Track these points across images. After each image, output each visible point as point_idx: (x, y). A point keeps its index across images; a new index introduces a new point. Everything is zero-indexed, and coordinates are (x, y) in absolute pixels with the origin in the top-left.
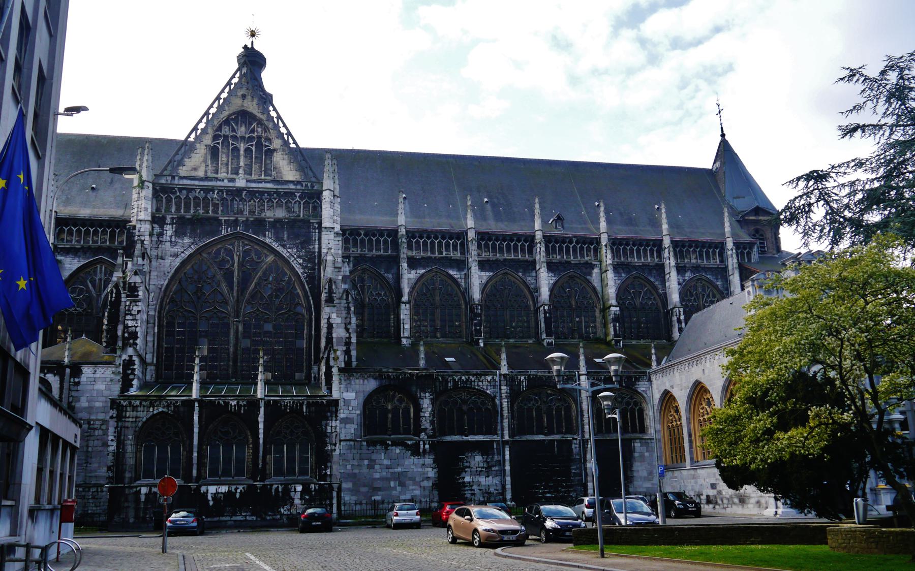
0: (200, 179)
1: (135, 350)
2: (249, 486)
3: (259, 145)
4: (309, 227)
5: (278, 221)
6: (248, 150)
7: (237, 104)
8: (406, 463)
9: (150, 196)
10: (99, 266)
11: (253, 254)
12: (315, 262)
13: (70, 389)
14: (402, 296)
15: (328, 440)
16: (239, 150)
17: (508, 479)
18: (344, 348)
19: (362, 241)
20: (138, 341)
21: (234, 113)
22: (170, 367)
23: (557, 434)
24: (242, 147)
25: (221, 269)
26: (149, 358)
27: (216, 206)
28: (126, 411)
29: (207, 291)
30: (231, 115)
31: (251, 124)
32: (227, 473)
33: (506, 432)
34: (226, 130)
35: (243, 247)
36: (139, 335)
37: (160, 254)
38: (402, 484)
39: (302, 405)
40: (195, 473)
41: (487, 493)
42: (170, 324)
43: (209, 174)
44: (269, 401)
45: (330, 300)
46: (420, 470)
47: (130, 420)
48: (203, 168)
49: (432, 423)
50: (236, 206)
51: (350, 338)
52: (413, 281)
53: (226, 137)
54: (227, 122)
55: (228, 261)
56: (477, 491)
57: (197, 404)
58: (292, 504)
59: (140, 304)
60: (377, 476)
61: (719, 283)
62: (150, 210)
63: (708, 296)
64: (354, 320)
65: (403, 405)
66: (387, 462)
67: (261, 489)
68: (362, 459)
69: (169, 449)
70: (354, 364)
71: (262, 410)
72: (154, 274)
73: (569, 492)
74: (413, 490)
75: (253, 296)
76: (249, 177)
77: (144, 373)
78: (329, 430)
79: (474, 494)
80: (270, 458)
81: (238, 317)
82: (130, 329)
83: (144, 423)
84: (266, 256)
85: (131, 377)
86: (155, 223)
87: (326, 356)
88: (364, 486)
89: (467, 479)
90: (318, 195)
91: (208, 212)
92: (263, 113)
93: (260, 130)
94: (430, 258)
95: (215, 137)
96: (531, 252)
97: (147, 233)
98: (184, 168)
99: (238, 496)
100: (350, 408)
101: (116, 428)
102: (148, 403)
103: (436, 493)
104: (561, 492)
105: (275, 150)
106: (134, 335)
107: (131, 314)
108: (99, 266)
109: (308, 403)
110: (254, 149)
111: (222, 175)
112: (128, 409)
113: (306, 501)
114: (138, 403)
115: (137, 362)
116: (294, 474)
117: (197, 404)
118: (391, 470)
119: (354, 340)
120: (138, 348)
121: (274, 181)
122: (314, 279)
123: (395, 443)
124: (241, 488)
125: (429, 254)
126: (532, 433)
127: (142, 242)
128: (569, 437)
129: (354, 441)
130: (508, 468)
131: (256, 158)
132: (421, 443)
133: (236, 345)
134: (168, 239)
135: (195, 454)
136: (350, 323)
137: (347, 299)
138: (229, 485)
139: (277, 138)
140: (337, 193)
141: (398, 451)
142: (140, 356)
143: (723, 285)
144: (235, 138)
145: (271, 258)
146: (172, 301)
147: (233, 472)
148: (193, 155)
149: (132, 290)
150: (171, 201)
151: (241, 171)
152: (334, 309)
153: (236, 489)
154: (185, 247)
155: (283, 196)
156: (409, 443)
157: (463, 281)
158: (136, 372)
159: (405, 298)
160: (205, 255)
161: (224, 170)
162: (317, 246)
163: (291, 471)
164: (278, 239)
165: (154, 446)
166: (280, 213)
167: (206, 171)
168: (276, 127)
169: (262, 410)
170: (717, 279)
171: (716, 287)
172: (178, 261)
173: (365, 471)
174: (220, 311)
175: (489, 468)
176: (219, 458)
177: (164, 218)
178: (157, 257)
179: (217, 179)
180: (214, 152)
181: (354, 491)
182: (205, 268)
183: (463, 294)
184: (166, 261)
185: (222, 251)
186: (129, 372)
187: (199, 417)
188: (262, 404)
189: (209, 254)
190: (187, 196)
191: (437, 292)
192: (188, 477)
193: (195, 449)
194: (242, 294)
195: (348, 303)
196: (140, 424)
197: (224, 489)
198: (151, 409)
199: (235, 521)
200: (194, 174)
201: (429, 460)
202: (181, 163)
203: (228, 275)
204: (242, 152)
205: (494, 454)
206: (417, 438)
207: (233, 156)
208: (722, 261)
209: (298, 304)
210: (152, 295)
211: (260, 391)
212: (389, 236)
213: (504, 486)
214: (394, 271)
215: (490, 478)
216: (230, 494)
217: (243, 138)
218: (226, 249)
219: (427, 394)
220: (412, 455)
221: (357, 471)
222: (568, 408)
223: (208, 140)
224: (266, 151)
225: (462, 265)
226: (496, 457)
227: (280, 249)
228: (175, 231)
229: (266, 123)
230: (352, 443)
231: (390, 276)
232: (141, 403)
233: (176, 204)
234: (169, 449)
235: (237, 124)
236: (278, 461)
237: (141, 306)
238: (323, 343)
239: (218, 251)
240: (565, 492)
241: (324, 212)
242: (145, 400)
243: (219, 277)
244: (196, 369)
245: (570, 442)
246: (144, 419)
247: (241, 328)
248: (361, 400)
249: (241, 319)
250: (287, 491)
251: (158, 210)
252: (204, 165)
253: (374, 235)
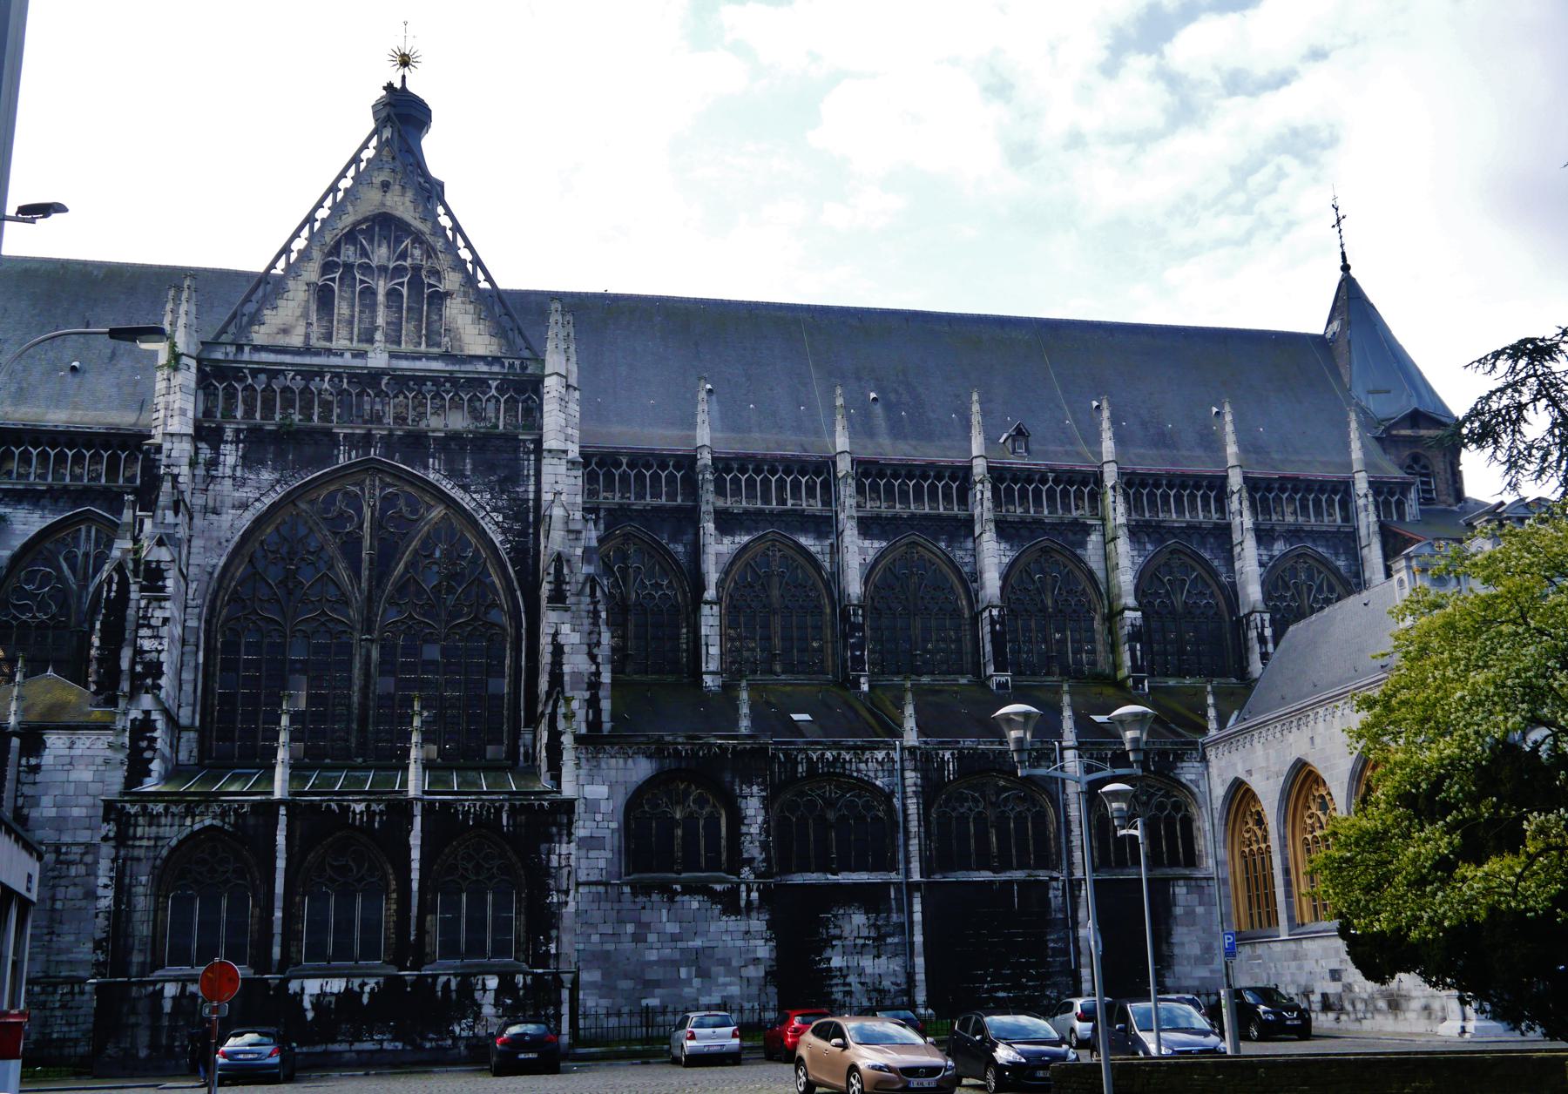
0: (296, 352)
1: (157, 698)
2: (388, 978)
3: (416, 284)
4: (516, 450)
5: (454, 437)
6: (393, 294)
7: (372, 201)
8: (712, 929)
9: (193, 385)
10: (83, 528)
11: (401, 503)
12: (528, 521)
13: (18, 781)
14: (704, 589)
15: (552, 882)
16: (374, 293)
17: (920, 961)
18: (587, 695)
19: (624, 478)
20: (163, 681)
21: (365, 220)
22: (230, 737)
23: (1020, 868)
24: (382, 287)
25: (335, 534)
26: (185, 715)
27: (326, 406)
28: (136, 825)
29: (307, 578)
30: (360, 222)
31: (399, 241)
32: (343, 952)
33: (915, 865)
34: (349, 254)
35: (382, 489)
36: (165, 668)
37: (211, 504)
38: (703, 974)
39: (499, 811)
40: (276, 952)
41: (875, 990)
42: (231, 646)
43: (314, 342)
44: (432, 803)
45: (558, 597)
46: (740, 943)
47: (145, 843)
48: (300, 330)
49: (764, 846)
50: (367, 407)
51: (598, 674)
52: (726, 559)
53: (348, 267)
54: (351, 236)
55: (351, 517)
56: (856, 987)
57: (283, 811)
58: (477, 1016)
59: (168, 604)
60: (652, 956)
62: (191, 414)
63: (1320, 589)
64: (606, 638)
65: (708, 809)
66: (673, 928)
67: (413, 984)
68: (621, 921)
69: (224, 903)
70: (607, 726)
71: (418, 821)
72: (195, 542)
73: (1043, 988)
74: (725, 985)
75: (401, 589)
76: (394, 347)
77: (175, 747)
78: (554, 863)
79: (849, 993)
80: (434, 922)
81: (369, 632)
82: (148, 657)
83: (173, 850)
84: (429, 508)
85: (148, 754)
86: (202, 440)
87: (549, 710)
88: (626, 976)
89: (837, 962)
90: (536, 384)
91: (311, 419)
92: (424, 220)
93: (417, 253)
94: (760, 512)
95: (327, 268)
96: (963, 499)
97: (186, 460)
98: (263, 329)
99: (365, 999)
100: (599, 817)
101: (113, 861)
102: (181, 808)
103: (772, 990)
104: (1026, 987)
105: (448, 294)
106: (155, 669)
107: (149, 626)
108: (83, 528)
109: (512, 806)
110: (405, 291)
111: (340, 343)
112: (141, 820)
113: (506, 1008)
114: (160, 808)
115: (160, 725)
116: (483, 954)
117: (283, 811)
118: (680, 945)
119: (606, 678)
120: (163, 694)
121: (447, 357)
122: (525, 555)
123: (689, 890)
124: (372, 983)
125: (759, 505)
126: (968, 868)
127: (175, 478)
128: (1043, 875)
129: (606, 884)
130: (918, 938)
131: (409, 309)
132: (743, 888)
133: (365, 689)
134: (228, 472)
135: (278, 914)
136: (598, 644)
137: (593, 594)
138: (349, 976)
139: (453, 269)
140: (573, 381)
141: (695, 905)
142: (166, 712)
143: (1349, 567)
144: (366, 268)
145: (438, 512)
146: (235, 598)
147: (357, 950)
148: (280, 303)
149: (153, 576)
150: (234, 396)
151: (378, 336)
152: (567, 616)
153: (362, 985)
154: (263, 488)
155: (462, 386)
156: (718, 887)
157: (827, 558)
158: (159, 744)
159: (710, 594)
160: (303, 506)
161: (344, 332)
162: (532, 488)
163: (476, 948)
164: (453, 474)
165: (192, 900)
166: (458, 421)
167: (307, 336)
168: (451, 247)
169: (418, 821)
170: (1337, 555)
171: (1335, 571)
172: (248, 518)
173: (627, 945)
174: (333, 619)
175: (880, 939)
176: (327, 921)
177: (220, 431)
178: (205, 509)
179: (329, 352)
180: (324, 298)
181: (606, 988)
182: (302, 531)
183: (827, 584)
184: (224, 517)
185: (339, 497)
186: (144, 744)
187: (287, 838)
188: (417, 810)
189: (312, 502)
190: (269, 385)
191: (776, 579)
192: (262, 962)
193: (279, 903)
194: (378, 586)
195: (595, 603)
196: (164, 853)
197: (337, 985)
198: (188, 821)
199: (359, 1052)
200: (282, 341)
201: (758, 924)
202: (255, 319)
203: (351, 547)
204: (381, 298)
205: (889, 911)
206: (734, 878)
207: (361, 305)
208: (1346, 519)
209: (494, 605)
210: (194, 586)
211: (415, 783)
212: (677, 467)
213: (910, 977)
214: (688, 538)
215: (884, 958)
216: (349, 996)
217: (383, 269)
218: (346, 493)
219: (755, 788)
220: (724, 912)
221: (610, 947)
222: (1041, 818)
223: (312, 273)
224: (430, 296)
225: (825, 526)
226: (894, 917)
227: (457, 494)
228: (244, 457)
229: (431, 239)
230: (601, 889)
231: (680, 548)
232: (166, 809)
233: (245, 402)
234: (224, 903)
235: (371, 241)
236: (449, 927)
237: (170, 609)
238: (543, 684)
239: (332, 495)
240: (1034, 988)
241: (546, 420)
242: (177, 803)
243: (332, 549)
244: (283, 737)
245: (1044, 886)
246: (174, 842)
247: (375, 654)
248: (621, 800)
249: (376, 635)
250: (467, 988)
251: (208, 413)
252: (302, 323)
253: (648, 467)
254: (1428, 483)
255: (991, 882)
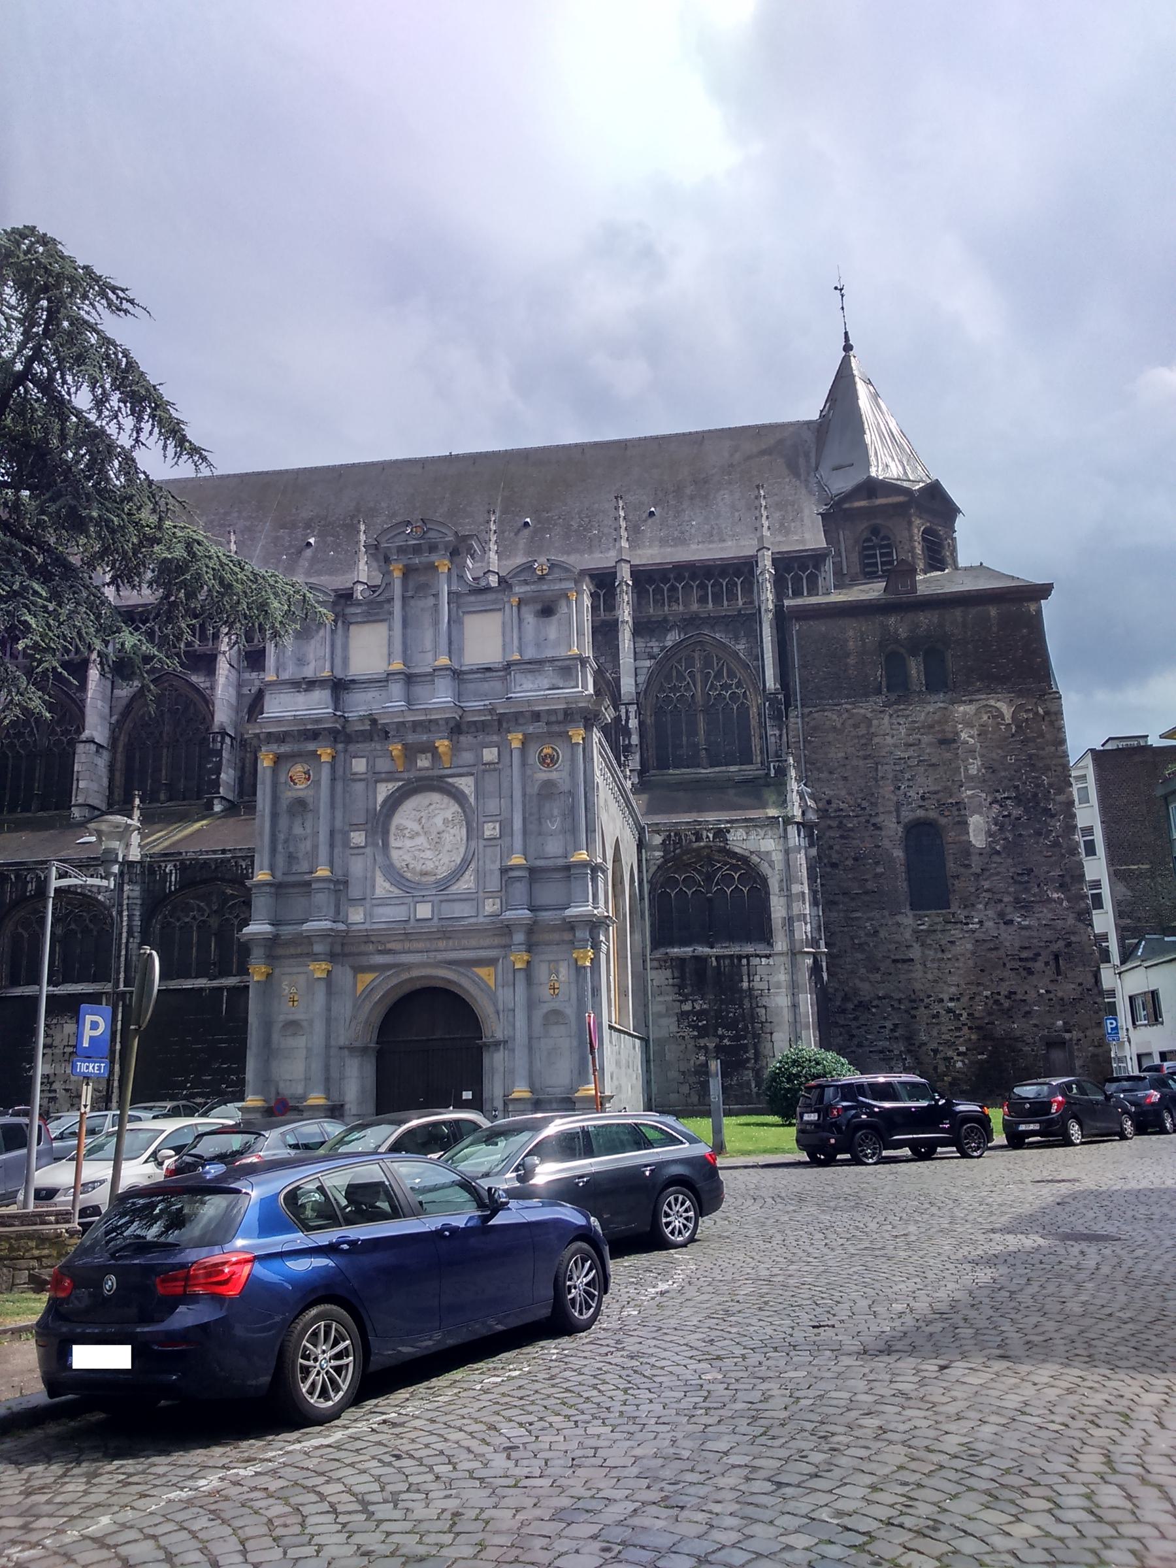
61: (741, 647)
63: (718, 676)
126: (187, 976)
143: (750, 652)
254: (890, 554)
255: (201, 989)
